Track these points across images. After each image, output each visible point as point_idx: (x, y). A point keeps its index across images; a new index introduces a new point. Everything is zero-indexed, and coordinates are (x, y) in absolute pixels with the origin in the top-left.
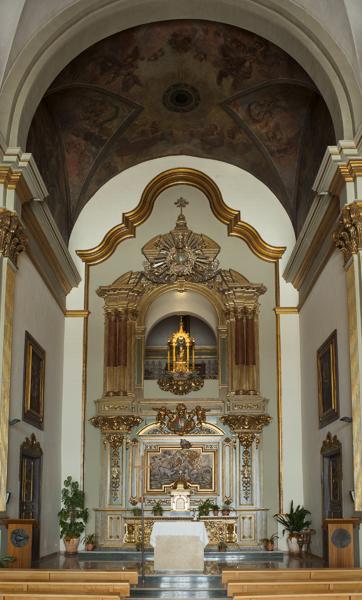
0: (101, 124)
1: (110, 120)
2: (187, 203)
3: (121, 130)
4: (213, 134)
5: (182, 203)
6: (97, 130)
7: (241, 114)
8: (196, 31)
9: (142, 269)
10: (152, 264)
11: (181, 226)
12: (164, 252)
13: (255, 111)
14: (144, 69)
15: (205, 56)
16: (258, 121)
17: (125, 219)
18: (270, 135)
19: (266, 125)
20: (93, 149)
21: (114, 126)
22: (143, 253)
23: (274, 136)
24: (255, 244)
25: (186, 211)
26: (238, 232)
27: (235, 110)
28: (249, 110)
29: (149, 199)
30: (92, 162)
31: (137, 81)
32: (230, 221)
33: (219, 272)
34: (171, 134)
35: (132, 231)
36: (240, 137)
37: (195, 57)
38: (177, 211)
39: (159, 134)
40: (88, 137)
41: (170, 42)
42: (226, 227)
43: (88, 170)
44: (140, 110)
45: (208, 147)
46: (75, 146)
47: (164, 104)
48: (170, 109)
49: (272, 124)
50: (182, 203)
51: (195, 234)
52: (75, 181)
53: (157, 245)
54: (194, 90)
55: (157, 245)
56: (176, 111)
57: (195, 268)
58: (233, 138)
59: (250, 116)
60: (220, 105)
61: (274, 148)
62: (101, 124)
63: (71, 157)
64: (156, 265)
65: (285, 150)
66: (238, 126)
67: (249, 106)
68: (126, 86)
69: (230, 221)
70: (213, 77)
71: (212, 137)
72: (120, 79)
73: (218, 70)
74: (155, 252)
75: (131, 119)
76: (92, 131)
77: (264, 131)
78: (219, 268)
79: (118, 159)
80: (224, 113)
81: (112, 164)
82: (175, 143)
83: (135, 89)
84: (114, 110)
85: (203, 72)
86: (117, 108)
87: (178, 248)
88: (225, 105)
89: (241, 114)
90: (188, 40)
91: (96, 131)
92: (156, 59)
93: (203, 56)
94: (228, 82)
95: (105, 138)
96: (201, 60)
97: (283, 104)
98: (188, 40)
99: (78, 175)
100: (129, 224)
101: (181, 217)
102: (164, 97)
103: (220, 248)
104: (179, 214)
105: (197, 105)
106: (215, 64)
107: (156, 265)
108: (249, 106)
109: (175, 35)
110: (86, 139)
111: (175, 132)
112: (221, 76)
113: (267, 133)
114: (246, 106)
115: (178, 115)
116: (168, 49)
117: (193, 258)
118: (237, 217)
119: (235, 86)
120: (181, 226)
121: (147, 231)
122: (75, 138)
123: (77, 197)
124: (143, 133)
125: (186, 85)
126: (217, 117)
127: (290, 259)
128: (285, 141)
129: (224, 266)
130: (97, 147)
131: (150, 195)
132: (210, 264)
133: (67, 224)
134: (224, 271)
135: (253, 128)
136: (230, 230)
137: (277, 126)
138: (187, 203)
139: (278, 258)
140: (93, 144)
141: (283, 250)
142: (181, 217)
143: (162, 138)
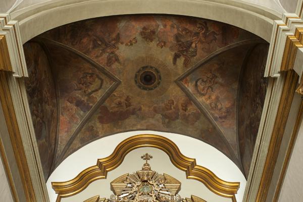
0: (90, 94)
1: (97, 90)
2: (151, 157)
3: (103, 100)
4: (171, 109)
5: (147, 157)
6: (86, 98)
7: (190, 88)
8: (159, 26)
11: (147, 167)
13: (201, 86)
14: (123, 51)
15: (165, 43)
16: (203, 95)
17: (99, 163)
18: (213, 105)
19: (210, 97)
20: (82, 113)
21: (98, 96)
23: (216, 106)
24: (210, 181)
26: (196, 175)
27: (187, 86)
28: (196, 85)
29: (121, 152)
30: (80, 122)
31: (117, 60)
32: (188, 168)
34: (140, 109)
35: (105, 174)
36: (192, 109)
37: (158, 45)
39: (131, 108)
40: (79, 104)
41: (142, 33)
42: (185, 172)
43: (75, 128)
44: (120, 83)
46: (68, 110)
47: (136, 82)
48: (140, 87)
49: (213, 97)
50: (147, 157)
52: (63, 136)
54: (157, 71)
56: (145, 89)
58: (185, 110)
59: (198, 91)
60: (175, 82)
61: (216, 115)
62: (90, 94)
63: (64, 118)
65: (225, 117)
66: (190, 99)
67: (197, 82)
68: (110, 62)
69: (188, 168)
70: (170, 58)
71: (170, 111)
73: (173, 53)
75: (112, 90)
76: (83, 99)
77: (208, 102)
79: (99, 125)
80: (179, 89)
81: (95, 128)
82: (143, 118)
83: (115, 66)
84: (100, 82)
85: (163, 56)
86: (102, 81)
88: (179, 82)
89: (190, 88)
90: (153, 32)
91: (85, 99)
92: (131, 44)
93: (162, 44)
94: (181, 61)
95: (91, 105)
96: (162, 47)
97: (220, 80)
98: (153, 32)
99: (67, 132)
100: (103, 168)
102: (136, 76)
105: (159, 83)
106: (171, 49)
108: (197, 82)
109: (144, 28)
110: (77, 105)
111: (143, 108)
112: (176, 57)
113: (211, 104)
114: (194, 83)
115: (145, 92)
116: (139, 38)
119: (186, 64)
120: (147, 167)
122: (69, 104)
123: (63, 147)
124: (120, 103)
125: (152, 67)
126: (174, 93)
127: (245, 194)
128: (224, 110)
130: (84, 112)
131: (122, 150)
133: (51, 163)
135: (201, 100)
137: (217, 98)
138: (151, 157)
139: (233, 193)
140: (82, 110)
141: (236, 186)
143: (133, 113)
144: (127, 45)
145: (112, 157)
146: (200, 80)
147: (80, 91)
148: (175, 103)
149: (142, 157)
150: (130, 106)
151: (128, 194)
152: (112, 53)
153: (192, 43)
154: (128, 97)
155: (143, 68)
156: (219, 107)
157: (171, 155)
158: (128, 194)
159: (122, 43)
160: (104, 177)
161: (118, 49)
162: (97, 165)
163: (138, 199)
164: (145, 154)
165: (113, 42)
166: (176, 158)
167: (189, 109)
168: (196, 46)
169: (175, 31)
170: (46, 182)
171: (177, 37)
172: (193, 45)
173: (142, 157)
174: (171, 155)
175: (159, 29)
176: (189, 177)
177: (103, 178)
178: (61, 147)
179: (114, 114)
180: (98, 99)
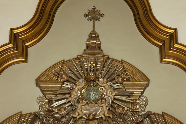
2: (102, 15)
9: (35, 108)
10: (50, 102)
11: (93, 46)
12: (68, 85)
17: (14, 37)
22: (38, 85)
25: (100, 27)
32: (163, 42)
33: (148, 115)
38: (88, 27)
42: (158, 49)
51: (113, 60)
53: (58, 75)
55: (58, 75)
57: (112, 108)
64: (56, 104)
69: (163, 42)
74: (54, 86)
78: (146, 110)
87: (88, 81)
101: (94, 36)
103: (148, 80)
104: (92, 30)
107: (56, 104)
117: (109, 95)
118: (173, 37)
120: (93, 46)
121: (47, 53)
129: (154, 107)
132: (134, 103)
134: (155, 114)
136: (163, 55)
138: (102, 15)
142: (94, 36)
145: (33, 22)
149: (86, 16)
151: (64, 101)
157: (136, 12)
158: (64, 101)
162: (10, 43)
163: (80, 112)
164: (91, 9)
166: (145, 22)
173: (86, 16)
174: (136, 12)
176: (164, 60)
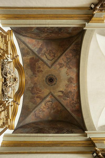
0: (45, 55)
1: (47, 58)
3: (42, 60)
4: (37, 91)
6: (43, 53)
8: (74, 84)
13: (49, 103)
15: (67, 87)
16: (45, 105)
19: (44, 108)
20: (37, 50)
21: (44, 58)
28: (49, 101)
30: (32, 48)
31: (61, 67)
36: (38, 100)
37: (66, 84)
39: (37, 73)
40: (40, 49)
41: (71, 78)
43: (30, 46)
44: (50, 68)
45: (31, 89)
46: (37, 44)
48: (47, 77)
49: (44, 109)
52: (27, 40)
54: (55, 84)
56: (46, 79)
58: (37, 97)
59: (47, 102)
60: (51, 92)
61: (36, 112)
62: (45, 55)
63: (34, 41)
65: (36, 116)
66: (43, 99)
67: (51, 101)
70: (61, 90)
71: (35, 91)
72: (63, 62)
73: (64, 91)
75: (47, 65)
76: (43, 51)
77: (42, 107)
79: (29, 57)
81: (28, 55)
83: (58, 66)
84: (51, 59)
86: (51, 60)
89: (48, 99)
90: (71, 82)
91: (43, 52)
92: (67, 73)
94: (60, 94)
95: (40, 54)
96: (66, 86)
97: (52, 111)
98: (71, 82)
99: (28, 42)
105: (49, 85)
106: (65, 90)
108: (51, 101)
109: (73, 79)
112: (62, 92)
113: (41, 109)
114: (51, 100)
116: (69, 76)
119: (59, 96)
122: (40, 44)
124: (40, 67)
125: (56, 82)
130: (37, 51)
135: (43, 104)
137: (44, 111)
144: (67, 71)
146: (52, 103)
147: (46, 50)
148: (40, 92)
150: (38, 72)
152: (64, 65)
153: (69, 98)
154: (43, 71)
155: (56, 78)
156: (40, 113)
159: (67, 70)
160: (12, 58)
161: (65, 68)
165: (68, 66)
167: (38, 99)
168: (68, 100)
169: (73, 91)
170: (10, 27)
171: (70, 92)
172: (68, 99)
175: (73, 84)
177: (11, 58)
178: (23, 38)
179: (35, 64)
180: (43, 58)
